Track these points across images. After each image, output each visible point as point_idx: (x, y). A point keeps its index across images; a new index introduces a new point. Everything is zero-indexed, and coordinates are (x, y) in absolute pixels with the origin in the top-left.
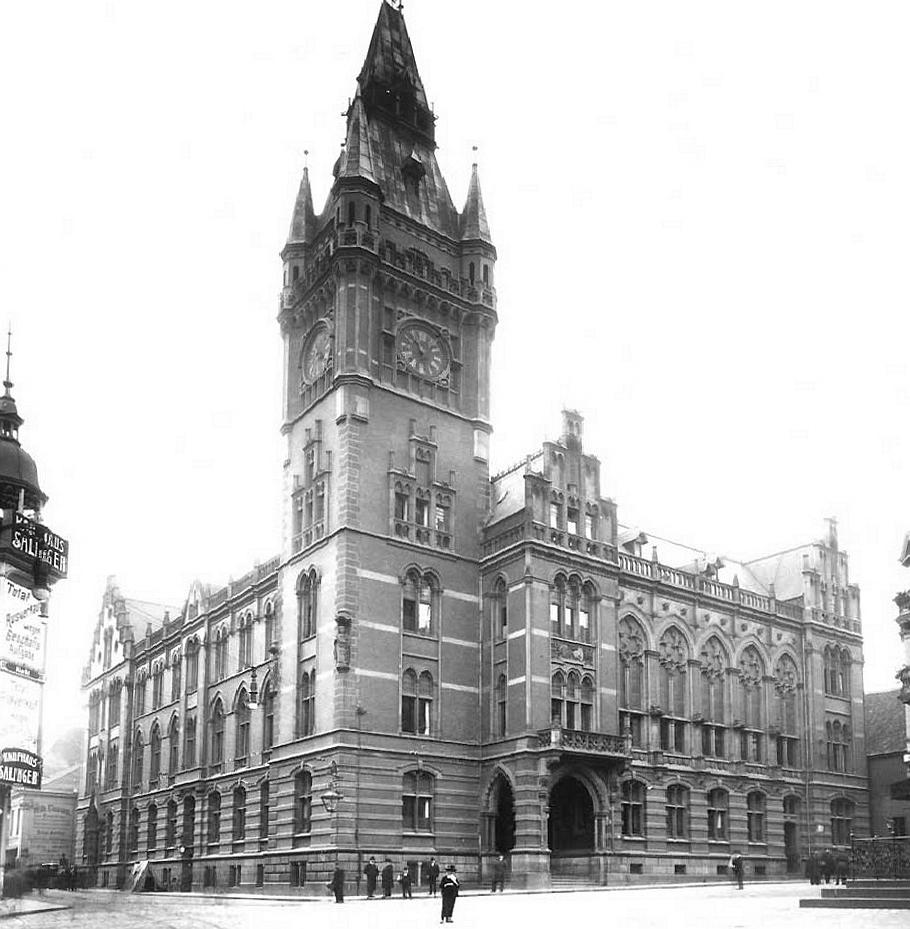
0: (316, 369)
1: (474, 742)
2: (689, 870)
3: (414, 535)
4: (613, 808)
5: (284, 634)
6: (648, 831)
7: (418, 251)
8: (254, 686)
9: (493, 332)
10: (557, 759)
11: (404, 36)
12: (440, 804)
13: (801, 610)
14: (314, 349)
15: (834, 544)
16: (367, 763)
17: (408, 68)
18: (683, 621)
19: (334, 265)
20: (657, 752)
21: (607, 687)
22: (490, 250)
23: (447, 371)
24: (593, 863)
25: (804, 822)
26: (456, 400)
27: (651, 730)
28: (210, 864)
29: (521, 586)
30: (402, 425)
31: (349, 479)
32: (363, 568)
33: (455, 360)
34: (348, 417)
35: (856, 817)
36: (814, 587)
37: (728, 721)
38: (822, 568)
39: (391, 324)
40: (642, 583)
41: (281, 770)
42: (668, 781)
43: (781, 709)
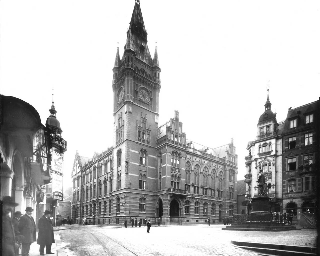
0: (121, 99)
1: (154, 191)
2: (199, 221)
3: (142, 141)
4: (184, 207)
5: (114, 165)
6: (191, 212)
7: (143, 69)
8: (108, 177)
9: (160, 90)
10: (172, 195)
11: (140, 12)
12: (147, 206)
13: (225, 160)
14: (120, 94)
15: (232, 144)
16: (132, 196)
17: (141, 20)
18: (199, 163)
19: (124, 73)
20: (193, 194)
21: (183, 178)
22: (159, 69)
23: (149, 100)
24: (179, 219)
25: (223, 210)
26: (151, 108)
27: (192, 189)
28: (99, 219)
29: (165, 154)
30: (139, 115)
31: (128, 127)
32: (131, 149)
33: (151, 97)
34: (128, 112)
35: (234, 210)
36: (228, 155)
37: (208, 187)
38: (230, 150)
39: (137, 88)
40: (191, 153)
41: (114, 197)
42: (195, 201)
43: (220, 185)
